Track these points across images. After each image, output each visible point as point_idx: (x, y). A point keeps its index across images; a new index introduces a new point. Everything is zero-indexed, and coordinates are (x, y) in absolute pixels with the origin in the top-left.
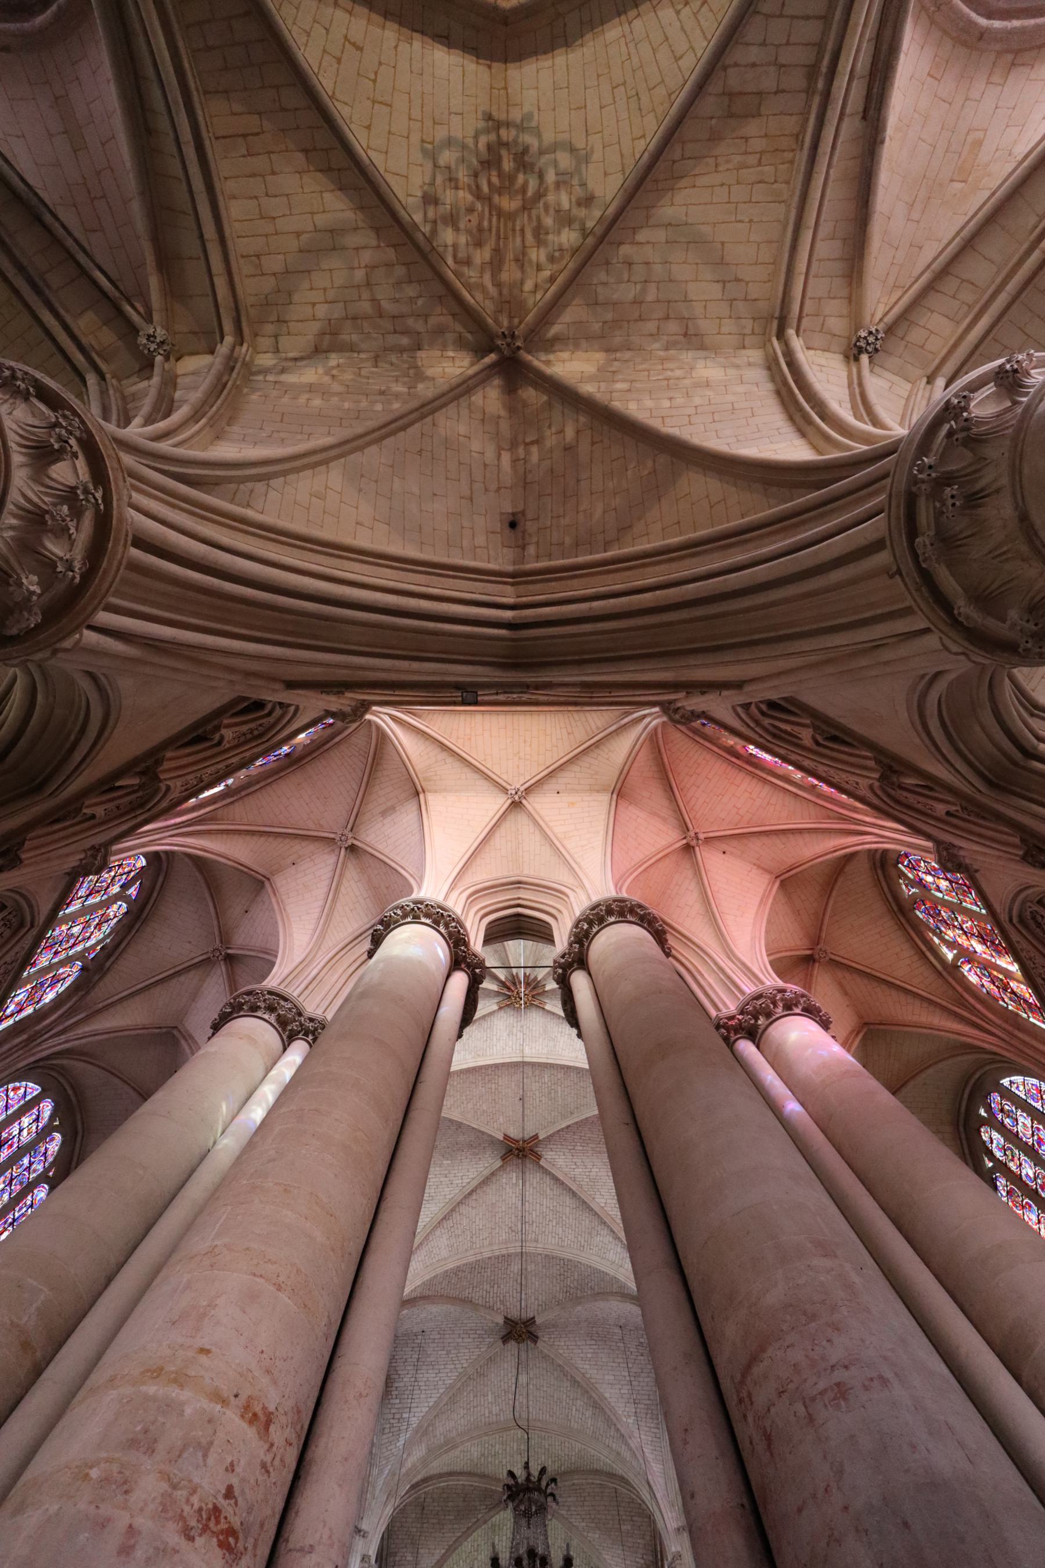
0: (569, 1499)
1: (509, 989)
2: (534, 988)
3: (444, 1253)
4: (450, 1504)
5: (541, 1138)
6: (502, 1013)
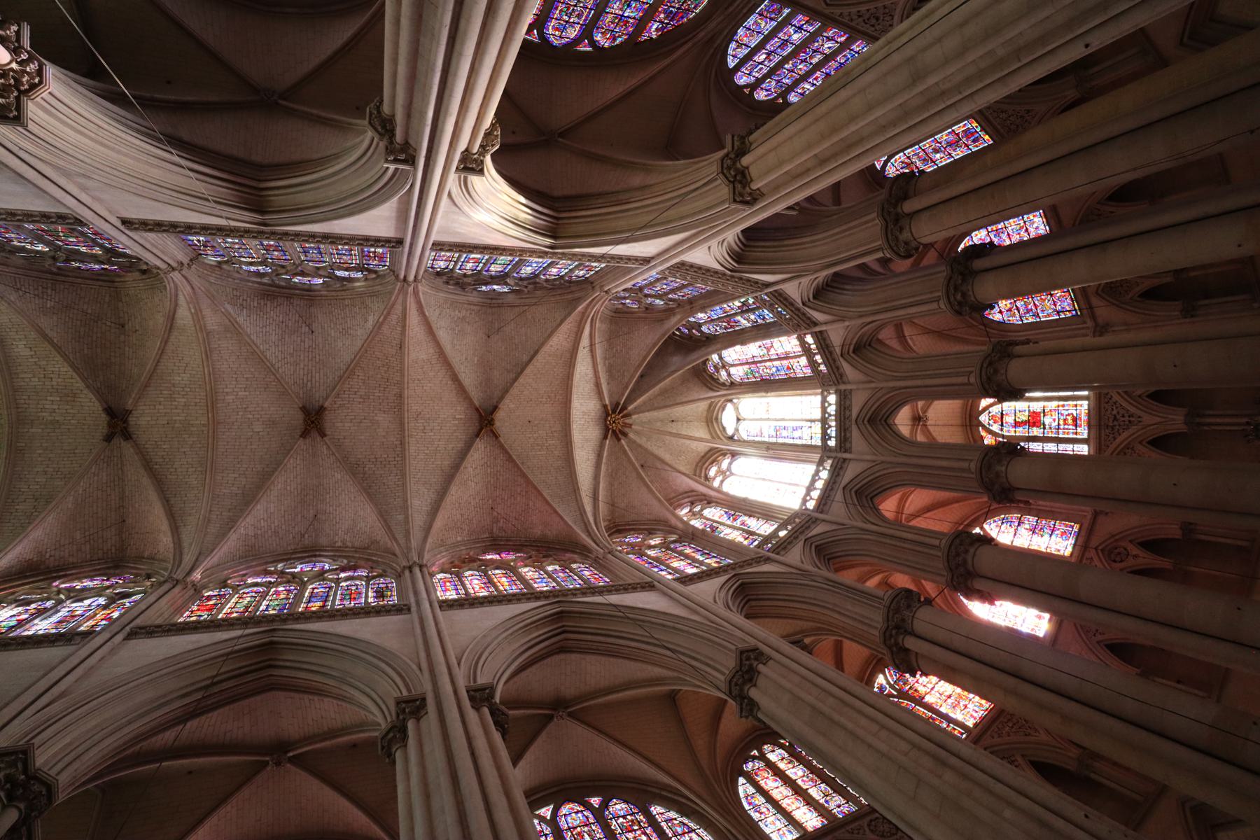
0: (104, 474)
3: (413, 356)
4: (99, 350)
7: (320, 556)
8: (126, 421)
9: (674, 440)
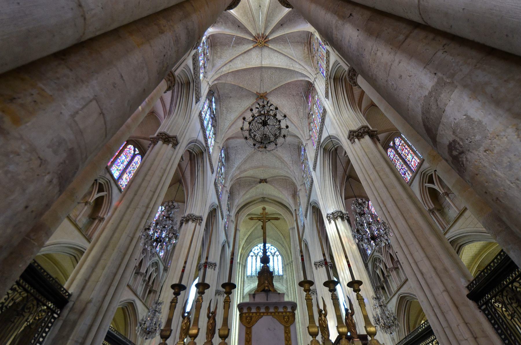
1: (257, 40)
2: (265, 39)
5: (268, 92)
6: (254, 50)
7: (300, 147)
8: (262, 180)
9: (271, 8)
